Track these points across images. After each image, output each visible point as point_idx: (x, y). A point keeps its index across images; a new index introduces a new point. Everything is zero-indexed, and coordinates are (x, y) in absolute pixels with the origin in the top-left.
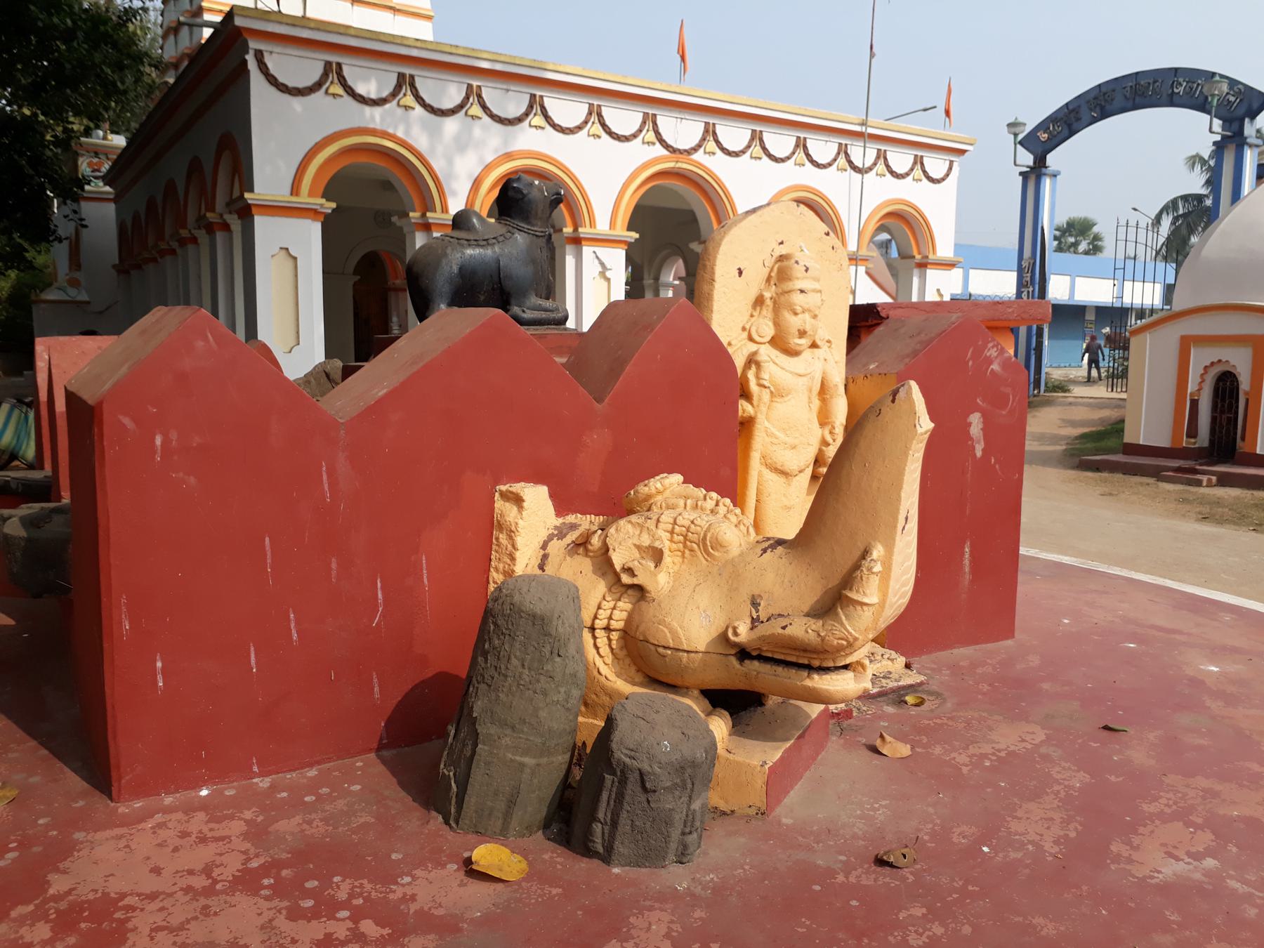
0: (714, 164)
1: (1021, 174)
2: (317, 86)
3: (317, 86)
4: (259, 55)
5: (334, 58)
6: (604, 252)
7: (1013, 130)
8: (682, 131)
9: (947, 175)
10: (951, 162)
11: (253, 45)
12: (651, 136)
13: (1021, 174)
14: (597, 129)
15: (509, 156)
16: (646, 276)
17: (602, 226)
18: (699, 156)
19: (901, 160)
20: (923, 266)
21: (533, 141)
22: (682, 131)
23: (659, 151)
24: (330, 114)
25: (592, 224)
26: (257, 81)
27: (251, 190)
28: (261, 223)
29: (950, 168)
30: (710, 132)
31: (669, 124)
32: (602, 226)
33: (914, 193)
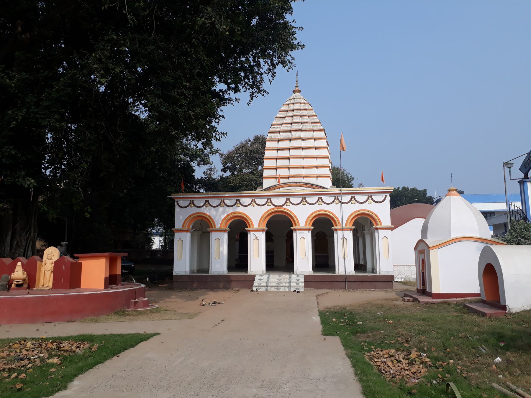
0: (290, 208)
1: (519, 182)
2: (188, 206)
3: (188, 206)
4: (177, 202)
5: (192, 200)
6: (257, 233)
7: (508, 166)
8: (279, 201)
9: (384, 200)
10: (386, 196)
11: (176, 200)
12: (270, 204)
13: (519, 182)
14: (254, 204)
15: (234, 213)
16: (359, 232)
17: (256, 226)
18: (285, 207)
19: (363, 198)
20: (377, 229)
21: (240, 209)
22: (279, 201)
23: (272, 207)
24: (193, 210)
25: (253, 226)
26: (177, 206)
27: (174, 227)
28: (176, 234)
29: (385, 198)
30: (288, 200)
31: (275, 201)
32: (256, 226)
33: (370, 207)
